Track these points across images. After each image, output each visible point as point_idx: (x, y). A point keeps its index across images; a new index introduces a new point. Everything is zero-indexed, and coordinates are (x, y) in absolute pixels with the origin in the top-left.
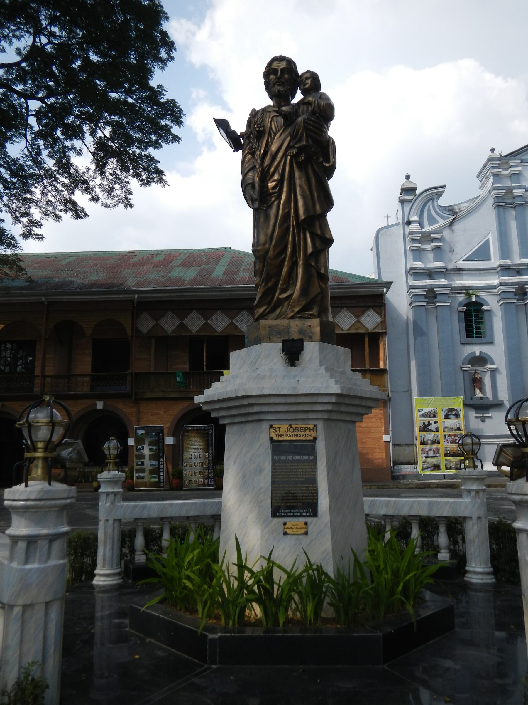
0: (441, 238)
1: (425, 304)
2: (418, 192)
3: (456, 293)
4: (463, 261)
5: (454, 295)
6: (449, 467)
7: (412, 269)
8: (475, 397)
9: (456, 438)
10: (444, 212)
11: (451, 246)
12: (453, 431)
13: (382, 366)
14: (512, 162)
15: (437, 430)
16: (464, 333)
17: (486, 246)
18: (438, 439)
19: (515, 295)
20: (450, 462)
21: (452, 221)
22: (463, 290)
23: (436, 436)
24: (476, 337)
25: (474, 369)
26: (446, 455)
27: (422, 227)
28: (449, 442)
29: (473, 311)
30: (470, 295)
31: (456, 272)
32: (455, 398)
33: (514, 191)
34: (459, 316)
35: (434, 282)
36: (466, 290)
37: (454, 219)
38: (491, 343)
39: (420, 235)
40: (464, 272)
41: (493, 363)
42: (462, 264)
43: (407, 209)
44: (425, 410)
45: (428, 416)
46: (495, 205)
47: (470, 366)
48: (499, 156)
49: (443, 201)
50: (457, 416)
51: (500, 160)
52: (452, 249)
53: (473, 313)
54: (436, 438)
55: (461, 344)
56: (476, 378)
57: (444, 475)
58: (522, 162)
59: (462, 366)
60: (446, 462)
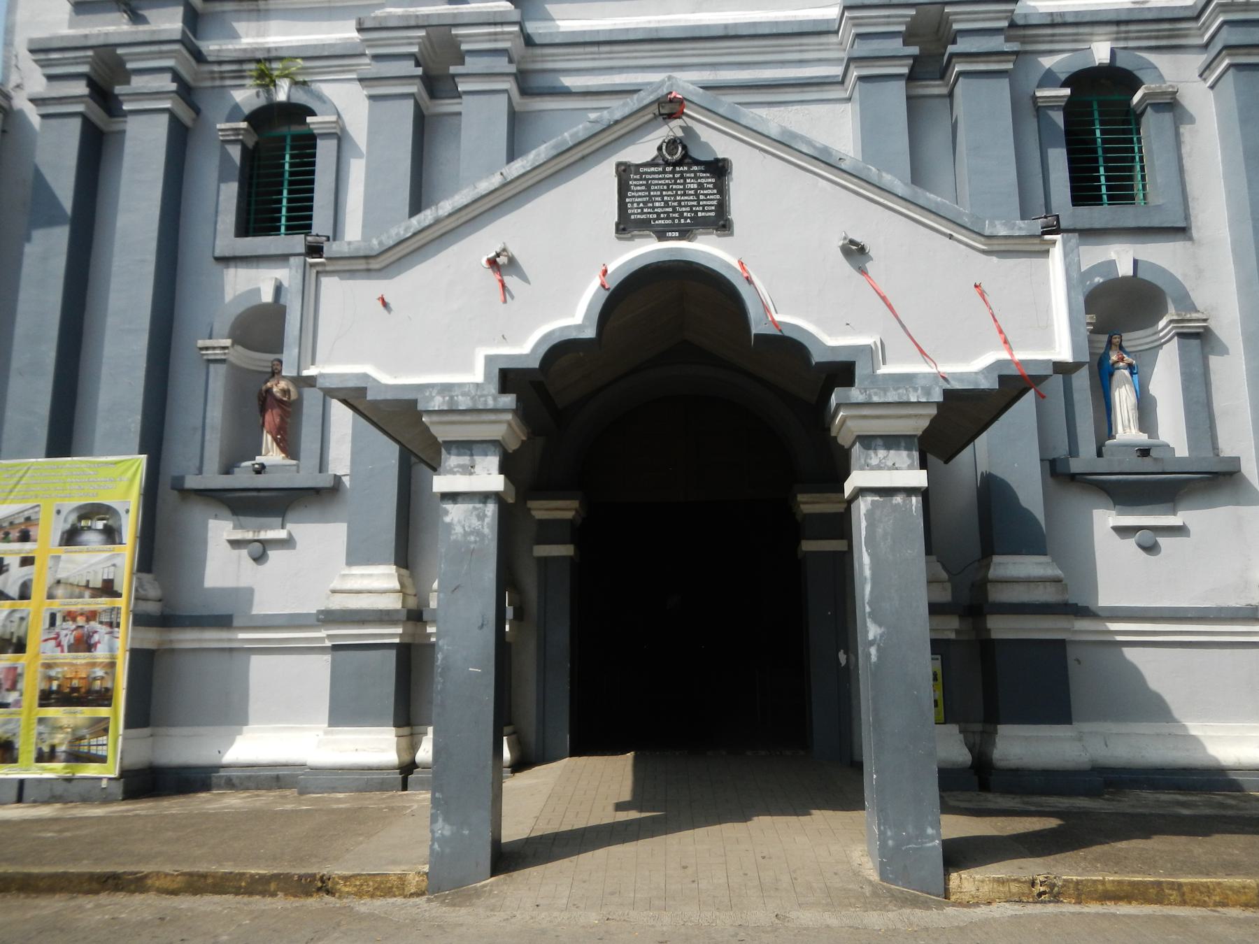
3: (222, 76)
5: (218, 83)
6: (46, 749)
9: (94, 625)
12: (87, 599)
15: (24, 594)
16: (228, 218)
18: (21, 633)
20: (56, 728)
23: (17, 616)
24: (286, 234)
26: (46, 698)
28: (65, 643)
29: (288, 141)
30: (266, 80)
32: (115, 463)
34: (225, 157)
50: (111, 535)
53: (288, 148)
54: (13, 628)
57: (22, 782)
59: (201, 343)
60: (42, 728)
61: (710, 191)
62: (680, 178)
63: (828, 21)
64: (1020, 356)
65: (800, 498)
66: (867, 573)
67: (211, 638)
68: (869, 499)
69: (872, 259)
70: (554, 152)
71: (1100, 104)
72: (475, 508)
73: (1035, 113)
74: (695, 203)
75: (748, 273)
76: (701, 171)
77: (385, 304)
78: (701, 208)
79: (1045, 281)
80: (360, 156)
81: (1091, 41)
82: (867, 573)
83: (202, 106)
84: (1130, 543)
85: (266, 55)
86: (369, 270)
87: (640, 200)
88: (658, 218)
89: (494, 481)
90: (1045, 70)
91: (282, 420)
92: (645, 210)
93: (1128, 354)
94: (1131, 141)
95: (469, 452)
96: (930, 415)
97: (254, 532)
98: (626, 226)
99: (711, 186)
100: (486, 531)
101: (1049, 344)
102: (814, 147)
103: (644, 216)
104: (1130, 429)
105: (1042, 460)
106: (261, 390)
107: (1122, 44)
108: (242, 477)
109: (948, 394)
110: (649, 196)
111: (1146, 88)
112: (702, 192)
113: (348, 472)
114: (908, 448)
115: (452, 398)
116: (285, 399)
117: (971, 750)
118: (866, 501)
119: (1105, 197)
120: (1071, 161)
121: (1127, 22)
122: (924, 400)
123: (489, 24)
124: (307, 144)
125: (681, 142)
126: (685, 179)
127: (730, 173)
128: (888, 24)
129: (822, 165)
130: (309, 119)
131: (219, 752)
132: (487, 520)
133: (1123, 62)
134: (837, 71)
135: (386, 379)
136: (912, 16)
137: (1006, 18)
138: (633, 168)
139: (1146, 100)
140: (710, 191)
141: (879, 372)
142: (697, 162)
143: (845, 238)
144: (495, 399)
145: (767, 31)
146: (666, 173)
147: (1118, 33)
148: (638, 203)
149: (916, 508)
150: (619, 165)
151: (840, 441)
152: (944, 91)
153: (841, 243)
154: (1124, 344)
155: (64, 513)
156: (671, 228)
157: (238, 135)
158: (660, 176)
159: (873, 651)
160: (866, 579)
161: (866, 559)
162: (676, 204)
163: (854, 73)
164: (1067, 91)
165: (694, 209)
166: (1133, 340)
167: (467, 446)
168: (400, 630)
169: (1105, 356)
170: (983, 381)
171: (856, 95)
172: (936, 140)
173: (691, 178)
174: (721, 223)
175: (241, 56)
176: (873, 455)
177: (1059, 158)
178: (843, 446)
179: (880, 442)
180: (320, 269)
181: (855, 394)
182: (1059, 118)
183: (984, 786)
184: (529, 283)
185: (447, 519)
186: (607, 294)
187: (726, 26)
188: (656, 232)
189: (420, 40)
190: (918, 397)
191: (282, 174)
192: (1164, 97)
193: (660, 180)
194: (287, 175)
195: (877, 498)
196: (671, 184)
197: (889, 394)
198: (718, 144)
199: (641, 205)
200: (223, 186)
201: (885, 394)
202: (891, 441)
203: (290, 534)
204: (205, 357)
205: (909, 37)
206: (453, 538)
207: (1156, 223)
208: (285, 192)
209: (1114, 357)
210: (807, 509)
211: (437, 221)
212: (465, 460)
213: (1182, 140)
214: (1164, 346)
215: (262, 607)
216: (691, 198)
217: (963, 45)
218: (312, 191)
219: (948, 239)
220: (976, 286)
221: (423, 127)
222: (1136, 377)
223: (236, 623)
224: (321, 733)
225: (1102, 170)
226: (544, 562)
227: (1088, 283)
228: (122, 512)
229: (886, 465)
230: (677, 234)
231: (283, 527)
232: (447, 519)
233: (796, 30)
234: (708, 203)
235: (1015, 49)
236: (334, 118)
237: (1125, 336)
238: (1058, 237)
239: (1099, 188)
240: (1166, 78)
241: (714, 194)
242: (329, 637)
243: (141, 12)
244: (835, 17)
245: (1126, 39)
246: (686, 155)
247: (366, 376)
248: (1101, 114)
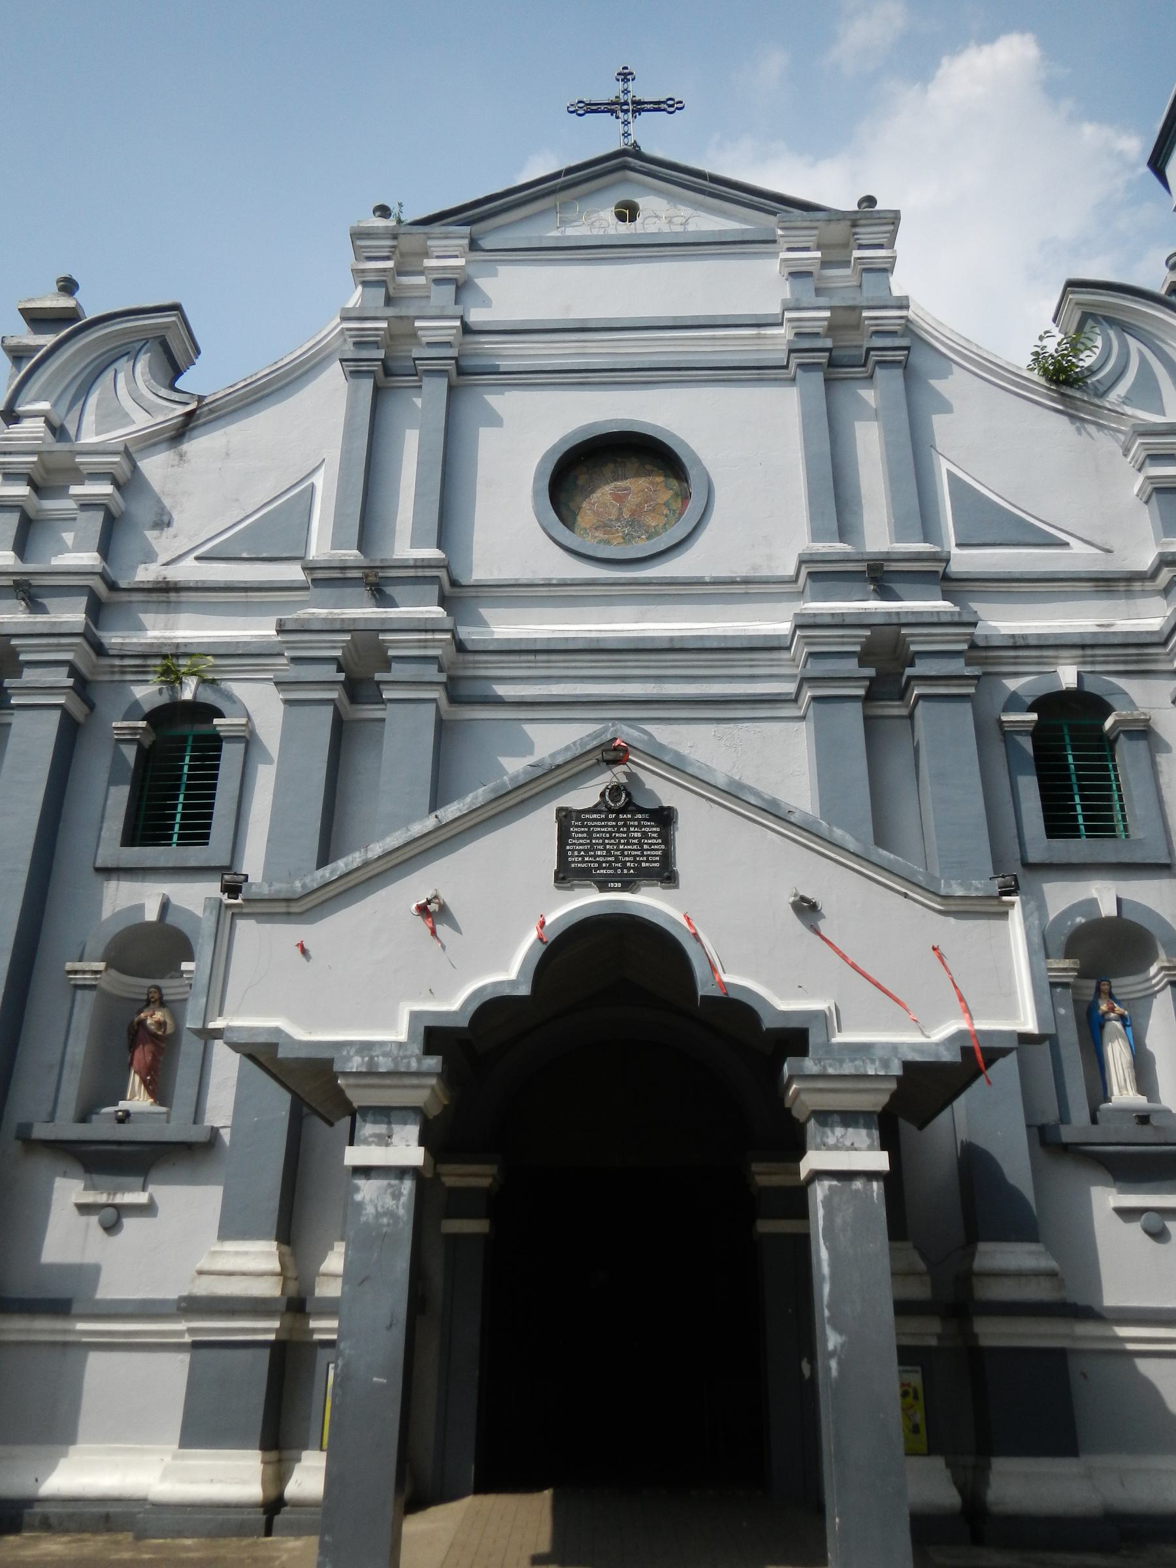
3: (123, 670)
4: (197, 558)
5: (117, 677)
11: (163, 508)
16: (114, 825)
19: (340, 670)
22: (155, 656)
24: (178, 845)
25: (139, 986)
29: (190, 740)
30: (171, 676)
31: (154, 597)
34: (118, 757)
37: (190, 415)
39: (35, 459)
40: (185, 596)
42: (188, 571)
47: (101, 966)
51: (395, 237)
52: (166, 519)
53: (189, 749)
58: (474, 246)
59: (69, 966)
61: (655, 841)
62: (623, 826)
63: (779, 637)
64: (982, 1025)
65: (755, 1167)
66: (826, 1270)
67: (43, 1328)
68: (827, 1183)
69: (824, 917)
70: (493, 796)
71: (1072, 728)
72: (390, 1186)
73: (1001, 737)
74: (639, 853)
75: (695, 930)
76: (645, 820)
77: (304, 951)
78: (645, 859)
79: (1006, 947)
80: (269, 761)
81: (1057, 664)
82: (826, 1270)
83: (95, 701)
84: (1135, 1229)
85: (174, 651)
86: (289, 914)
87: (581, 847)
88: (600, 868)
89: (415, 1155)
90: (1009, 694)
91: (155, 1058)
92: (587, 859)
93: (1118, 1002)
94: (1106, 768)
95: (386, 1120)
96: (889, 1089)
97: (109, 1194)
98: (566, 875)
99: (655, 835)
100: (401, 1212)
101: (1012, 1012)
102: (763, 799)
103: (585, 865)
104: (1127, 1090)
105: (1029, 1126)
106: (133, 1022)
107: (1088, 668)
108: (101, 1128)
109: (907, 1066)
110: (591, 844)
111: (1116, 714)
112: (646, 841)
113: (229, 1123)
114: (868, 1126)
115: (372, 1058)
116: (159, 1033)
117: (961, 1491)
118: (823, 1186)
119: (1082, 828)
120: (1042, 788)
121: (1093, 646)
122: (882, 1073)
124: (211, 746)
125: (625, 789)
126: (628, 827)
127: (676, 822)
128: (843, 644)
129: (771, 817)
130: (216, 721)
131: (37, 1480)
132: (403, 1199)
133: (1091, 686)
134: (790, 688)
135: (301, 1035)
136: (866, 637)
137: (965, 641)
138: (574, 815)
139: (1118, 727)
140: (655, 841)
141: (834, 1040)
142: (642, 810)
143: (796, 895)
144: (419, 1061)
145: (715, 645)
146: (610, 820)
147: (1084, 656)
148: (579, 851)
149: (877, 1194)
150: (559, 810)
151: (795, 1113)
152: (904, 712)
153: (792, 899)
154: (1114, 991)
156: (614, 878)
157: (136, 734)
158: (603, 823)
159: (833, 1364)
160: (823, 1277)
161: (824, 1254)
162: (619, 853)
163: (808, 693)
164: (1034, 716)
165: (638, 859)
166: (1124, 986)
167: (385, 1114)
168: (276, 1324)
169: (1093, 1007)
170: (944, 1053)
171: (811, 713)
172: (897, 764)
173: (635, 826)
174: (665, 874)
175: (147, 650)
176: (829, 1133)
177: (1029, 787)
178: (798, 1120)
179: (836, 1118)
180: (236, 910)
181: (809, 1065)
182: (1027, 744)
183: (978, 1539)
184: (461, 934)
185: (358, 1197)
186: (544, 947)
187: (672, 639)
188: (596, 882)
189: (345, 644)
190: (876, 1069)
191: (180, 777)
192: (1136, 724)
193: (602, 829)
194: (185, 777)
195: (835, 1183)
196: (614, 832)
197: (844, 1066)
198: (666, 793)
199: (582, 853)
200: (113, 789)
201: (841, 1066)
202: (849, 1118)
203: (151, 1198)
204: (73, 982)
205: (864, 658)
206: (363, 1219)
207: (1138, 858)
208: (181, 797)
209: (1104, 1007)
210: (762, 1181)
211: (366, 864)
212: (381, 1129)
213: (1159, 768)
214: (1158, 995)
215: (109, 1290)
216: (635, 847)
217: (922, 668)
218: (213, 796)
219: (903, 897)
220: (934, 949)
221: (341, 730)
222: (1129, 1029)
223: (76, 1308)
224: (168, 1459)
225: (1077, 798)
226: (454, 1240)
227: (1069, 923)
229: (844, 1145)
230: (620, 885)
231: (144, 1189)
232: (358, 1197)
233: (745, 645)
234: (653, 853)
235: (977, 673)
236: (243, 721)
237: (1115, 982)
238: (1015, 899)
239: (1075, 818)
240: (1138, 704)
241: (658, 844)
242: (191, 1331)
243: (40, 600)
244: (787, 633)
245: (1093, 663)
246: (630, 802)
247: (278, 1031)
248: (1072, 739)
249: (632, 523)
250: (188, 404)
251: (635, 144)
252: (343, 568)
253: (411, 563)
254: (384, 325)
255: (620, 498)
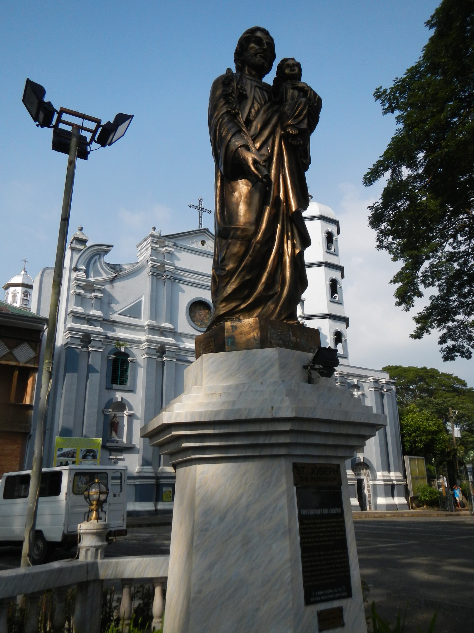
0: (103, 290)
1: (80, 347)
2: (88, 244)
3: (108, 342)
4: (118, 314)
7: (72, 312)
8: (111, 439)
10: (108, 268)
13: (27, 401)
14: (167, 243)
17: (139, 304)
19: (157, 352)
21: (114, 278)
22: (115, 340)
24: (120, 384)
27: (88, 276)
28: (83, 482)
29: (120, 360)
30: (120, 345)
31: (111, 323)
33: (166, 266)
35: (91, 328)
36: (117, 341)
37: (116, 276)
38: (132, 391)
39: (85, 283)
40: (118, 324)
41: (131, 408)
43: (76, 256)
44: (65, 450)
45: (67, 456)
46: (150, 273)
48: (159, 235)
49: (108, 258)
50: (94, 457)
51: (159, 239)
52: (110, 302)
55: (106, 388)
56: (115, 421)
58: (175, 245)
59: (104, 410)
123: (173, 346)
155: (82, 451)
228: (97, 452)
249: (202, 321)
250: (116, 273)
251: (208, 229)
252: (155, 327)
253: (169, 328)
254: (159, 264)
255: (200, 315)
